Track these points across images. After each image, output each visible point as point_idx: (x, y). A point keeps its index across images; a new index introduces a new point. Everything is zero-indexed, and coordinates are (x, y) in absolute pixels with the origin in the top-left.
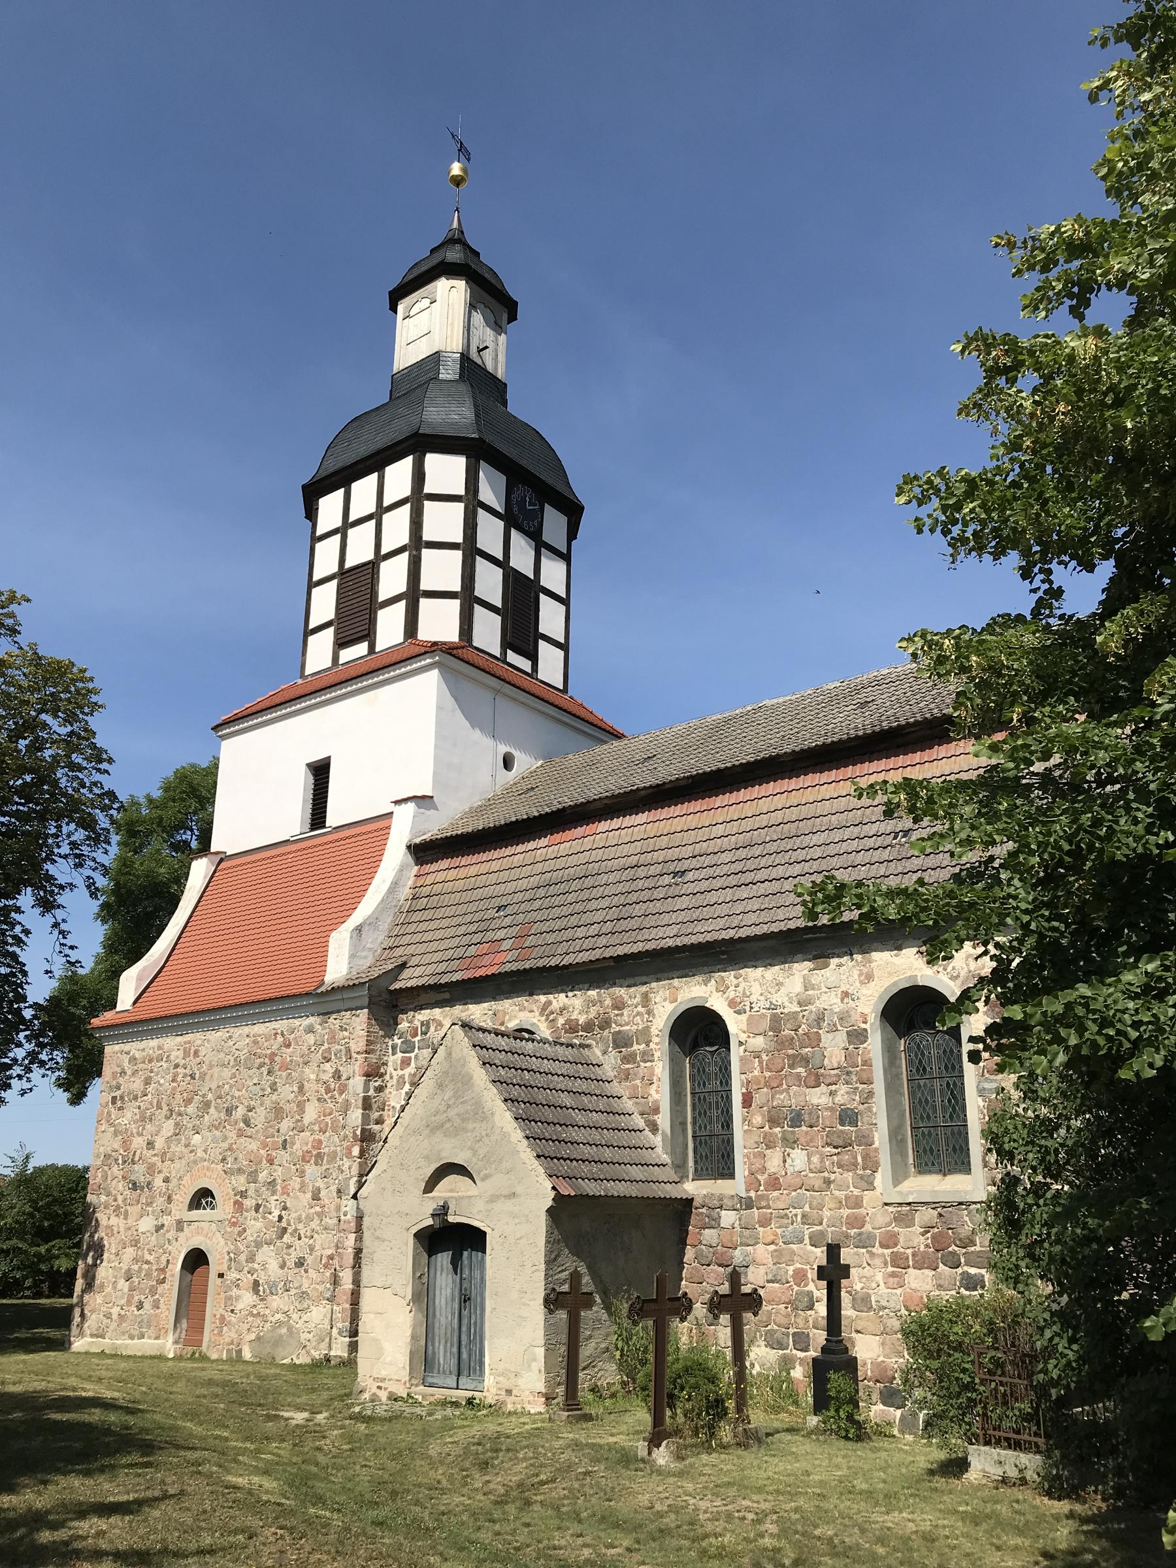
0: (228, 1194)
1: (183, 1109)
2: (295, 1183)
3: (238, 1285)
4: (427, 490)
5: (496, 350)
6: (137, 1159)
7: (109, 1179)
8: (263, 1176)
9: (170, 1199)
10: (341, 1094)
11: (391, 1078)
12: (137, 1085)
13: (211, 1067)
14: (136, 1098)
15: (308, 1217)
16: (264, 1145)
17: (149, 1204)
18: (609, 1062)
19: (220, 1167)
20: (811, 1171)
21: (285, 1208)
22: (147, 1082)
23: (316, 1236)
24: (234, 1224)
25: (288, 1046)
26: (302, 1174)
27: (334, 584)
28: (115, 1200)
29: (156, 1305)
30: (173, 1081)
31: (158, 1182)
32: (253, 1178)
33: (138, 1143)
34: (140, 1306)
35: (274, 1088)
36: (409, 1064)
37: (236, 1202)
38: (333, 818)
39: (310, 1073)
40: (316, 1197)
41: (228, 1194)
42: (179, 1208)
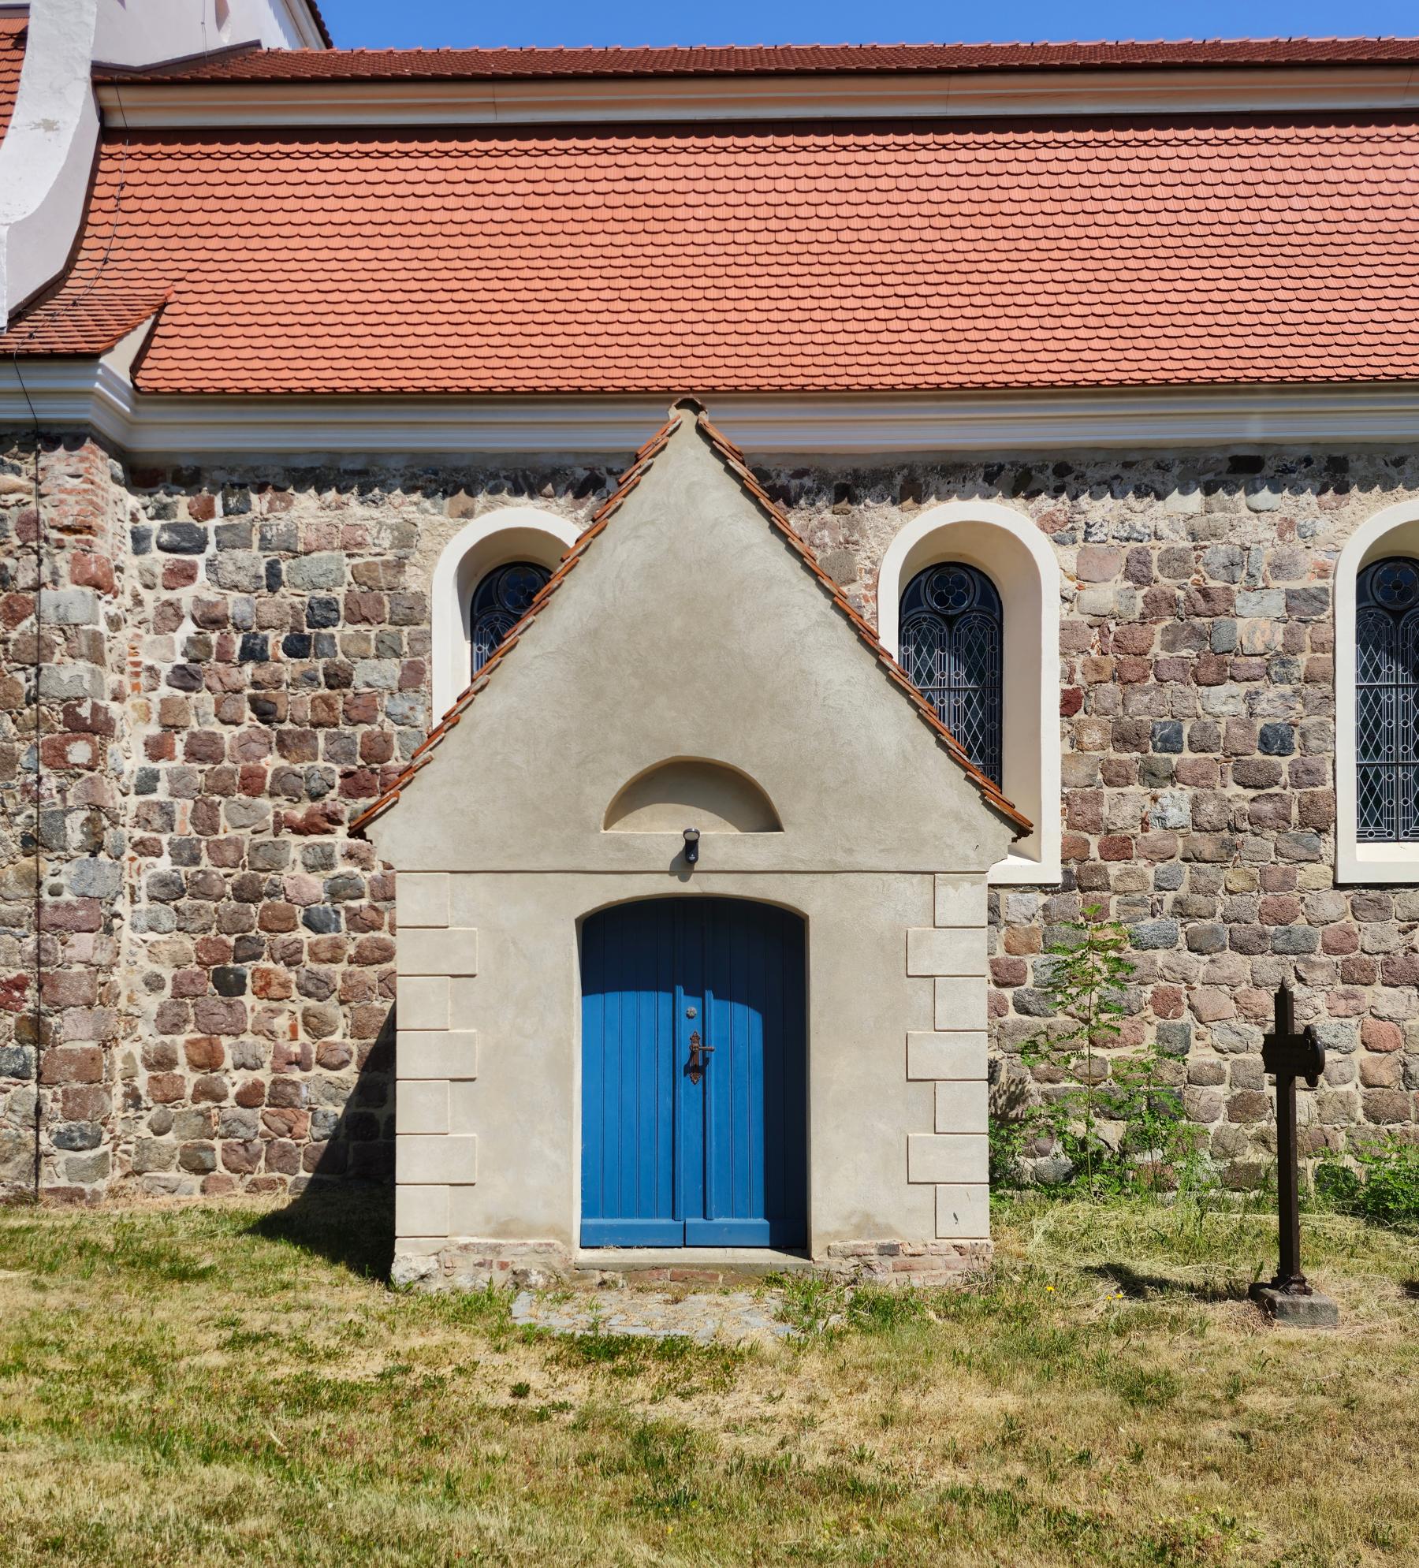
20: (1198, 827)
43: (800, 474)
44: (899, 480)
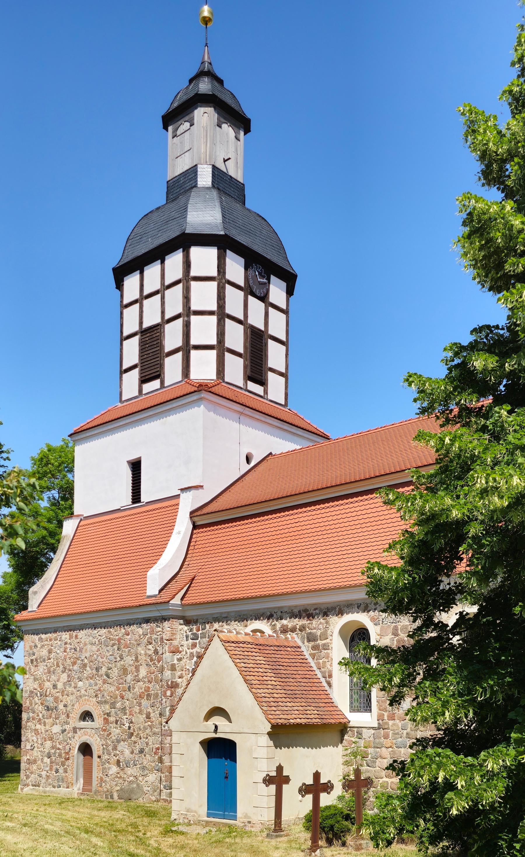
0: (100, 714)
1: (71, 667)
2: (137, 709)
3: (109, 762)
4: (193, 273)
5: (237, 159)
6: (48, 694)
7: (33, 704)
8: (118, 705)
9: (68, 716)
10: (159, 662)
11: (186, 653)
12: (44, 653)
13: (85, 644)
14: (44, 661)
15: (144, 727)
16: (118, 689)
17: (57, 718)
18: (306, 649)
19: (94, 699)
21: (132, 722)
22: (50, 652)
23: (149, 737)
24: (105, 730)
25: (128, 635)
26: (140, 705)
27: (137, 339)
28: (38, 716)
29: (66, 771)
30: (65, 651)
31: (61, 706)
32: (113, 705)
33: (48, 685)
34: (57, 771)
35: (122, 658)
36: (196, 646)
37: (105, 719)
38: (145, 497)
39: (141, 650)
40: (148, 717)
41: (100, 714)
42: (75, 721)
43: (315, 609)
44: (337, 609)
